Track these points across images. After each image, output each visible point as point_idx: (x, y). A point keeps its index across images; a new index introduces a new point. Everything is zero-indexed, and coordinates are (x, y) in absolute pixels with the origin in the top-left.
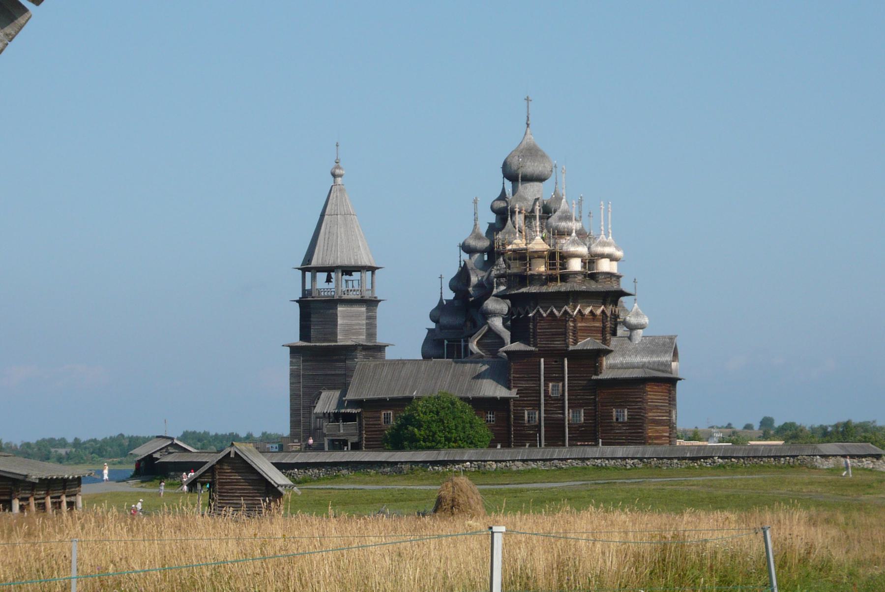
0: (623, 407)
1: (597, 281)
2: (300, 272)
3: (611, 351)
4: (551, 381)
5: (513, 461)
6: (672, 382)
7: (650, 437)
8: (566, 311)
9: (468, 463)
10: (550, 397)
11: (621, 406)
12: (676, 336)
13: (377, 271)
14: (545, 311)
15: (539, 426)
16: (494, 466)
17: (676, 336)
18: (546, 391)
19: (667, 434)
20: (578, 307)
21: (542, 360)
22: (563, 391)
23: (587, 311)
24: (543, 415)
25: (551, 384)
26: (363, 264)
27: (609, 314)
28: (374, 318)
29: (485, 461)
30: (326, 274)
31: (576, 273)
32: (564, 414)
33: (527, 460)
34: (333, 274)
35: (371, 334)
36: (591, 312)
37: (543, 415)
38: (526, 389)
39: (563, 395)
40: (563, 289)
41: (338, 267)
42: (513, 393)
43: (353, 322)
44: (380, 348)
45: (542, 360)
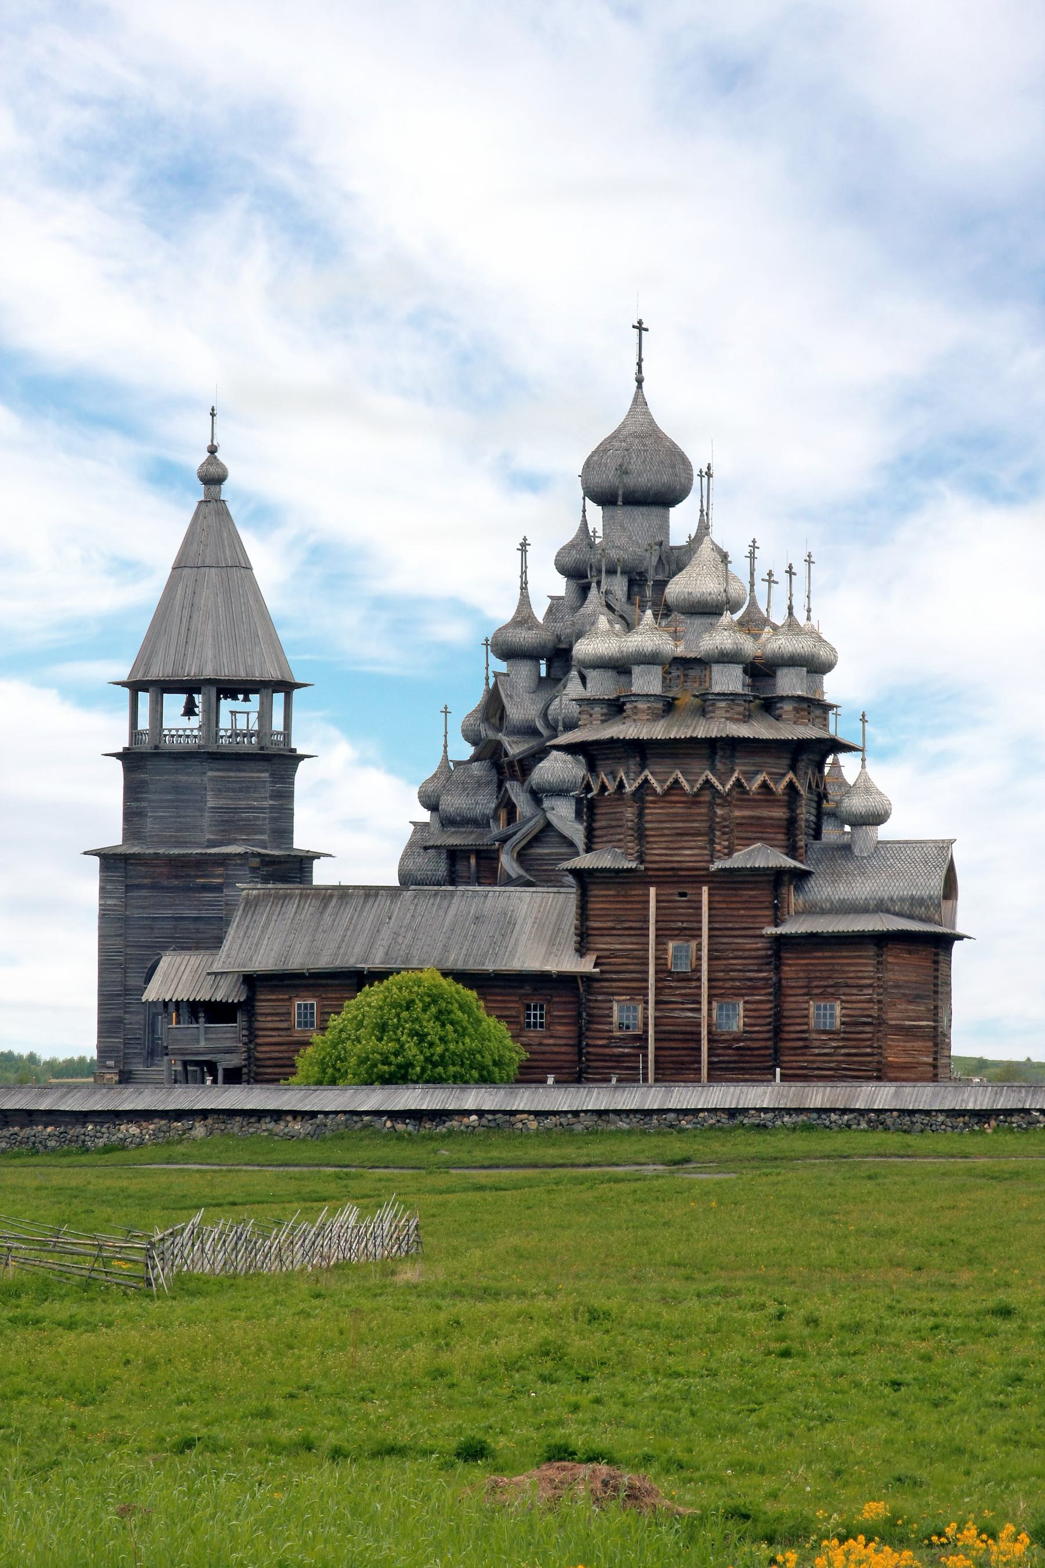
0: (834, 996)
1: (778, 718)
2: (127, 691)
5: (576, 1113)
6: (942, 943)
7: (891, 1065)
9: (474, 1117)
10: (670, 973)
12: (952, 842)
13: (296, 693)
14: (661, 782)
15: (643, 1038)
16: (533, 1125)
17: (952, 842)
19: (930, 1060)
20: (736, 775)
21: (652, 891)
22: (699, 958)
24: (651, 1012)
25: (671, 945)
26: (266, 677)
28: (289, 795)
29: (513, 1113)
30: (183, 698)
32: (699, 1010)
33: (606, 1112)
34: (198, 698)
35: (284, 831)
36: (764, 785)
37: (651, 1012)
40: (701, 733)
41: (210, 682)
42: (586, 966)
43: (243, 803)
44: (303, 863)
45: (652, 891)
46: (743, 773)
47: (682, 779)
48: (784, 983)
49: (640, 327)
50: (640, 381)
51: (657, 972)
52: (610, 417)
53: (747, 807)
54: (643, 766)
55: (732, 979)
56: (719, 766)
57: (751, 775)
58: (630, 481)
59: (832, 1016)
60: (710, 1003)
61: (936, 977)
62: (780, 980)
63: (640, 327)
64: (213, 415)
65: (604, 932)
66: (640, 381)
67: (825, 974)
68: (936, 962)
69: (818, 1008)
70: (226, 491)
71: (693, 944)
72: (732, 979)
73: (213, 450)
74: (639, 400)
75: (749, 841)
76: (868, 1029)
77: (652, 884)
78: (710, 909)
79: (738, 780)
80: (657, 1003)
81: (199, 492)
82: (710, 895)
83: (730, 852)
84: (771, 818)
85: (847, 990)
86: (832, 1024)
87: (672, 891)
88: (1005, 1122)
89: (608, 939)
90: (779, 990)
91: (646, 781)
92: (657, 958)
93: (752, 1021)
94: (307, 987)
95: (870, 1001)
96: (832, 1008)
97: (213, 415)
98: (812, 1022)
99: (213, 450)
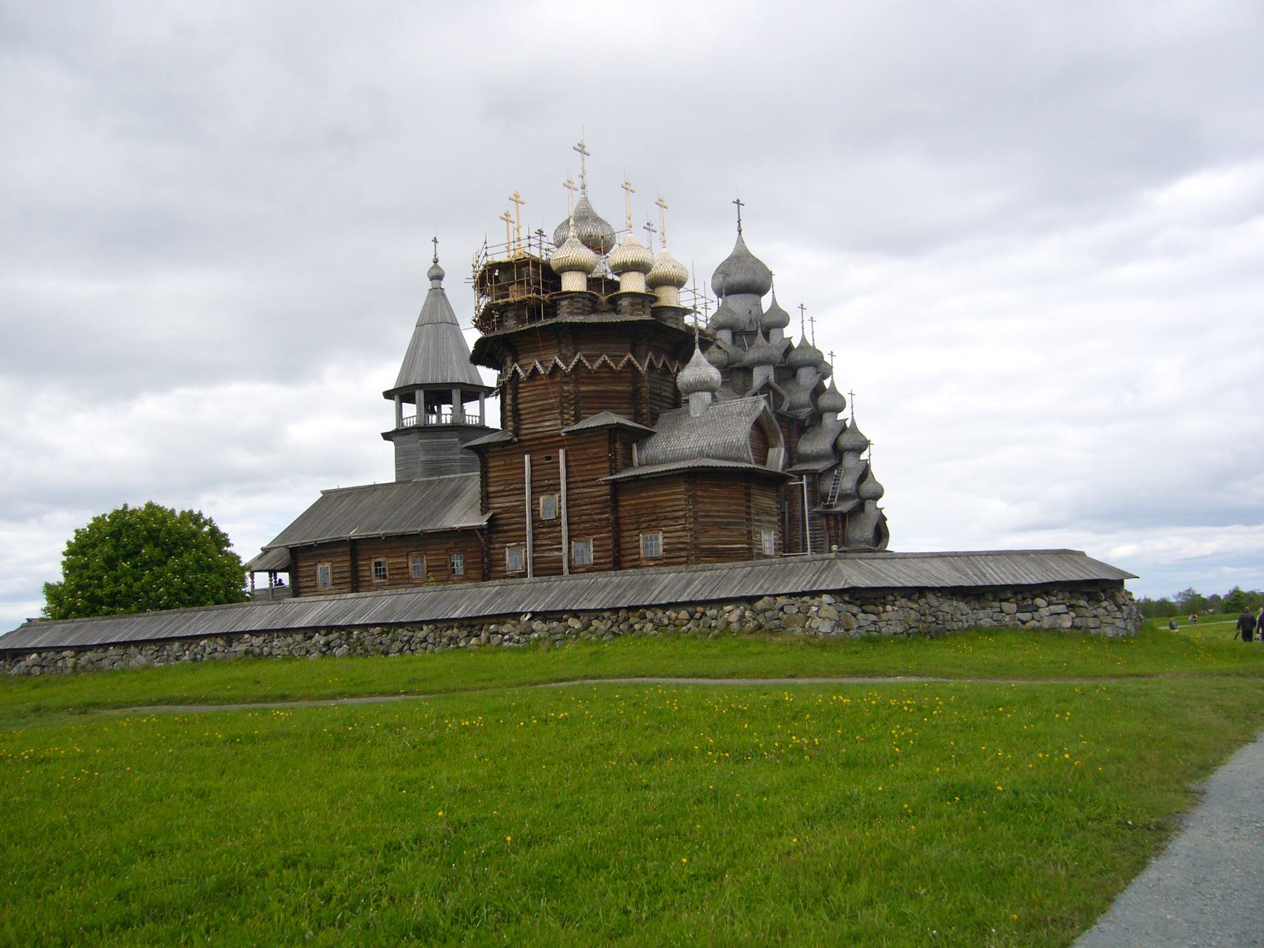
0: (657, 528)
3: (652, 434)
4: (543, 493)
5: (105, 646)
8: (556, 365)
9: (34, 656)
11: (653, 526)
18: (534, 511)
23: (599, 362)
25: (541, 499)
27: (643, 369)
31: (571, 295)
32: (560, 549)
38: (507, 510)
39: (559, 517)
43: (442, 457)
46: (585, 356)
47: (539, 366)
48: (622, 521)
49: (738, 202)
50: (740, 231)
51: (533, 522)
52: (725, 251)
53: (595, 384)
54: (515, 360)
55: (584, 522)
56: (564, 351)
57: (591, 359)
58: (730, 280)
59: (657, 545)
60: (570, 543)
61: (749, 507)
62: (617, 519)
63: (738, 202)
64: (435, 241)
65: (498, 494)
66: (740, 231)
67: (650, 511)
68: (748, 494)
69: (646, 539)
70: (444, 284)
71: (557, 496)
72: (584, 522)
73: (436, 262)
74: (740, 241)
75: (596, 410)
76: (683, 554)
77: (527, 453)
78: (567, 467)
79: (579, 361)
80: (534, 546)
81: (429, 285)
82: (567, 456)
83: (577, 421)
84: (616, 392)
85: (665, 522)
86: (657, 551)
87: (540, 457)
88: (497, 633)
89: (500, 500)
90: (617, 529)
91: (515, 372)
92: (533, 511)
93: (601, 554)
94: (324, 556)
95: (684, 530)
96: (657, 539)
97: (435, 241)
98: (642, 551)
99: (436, 262)
